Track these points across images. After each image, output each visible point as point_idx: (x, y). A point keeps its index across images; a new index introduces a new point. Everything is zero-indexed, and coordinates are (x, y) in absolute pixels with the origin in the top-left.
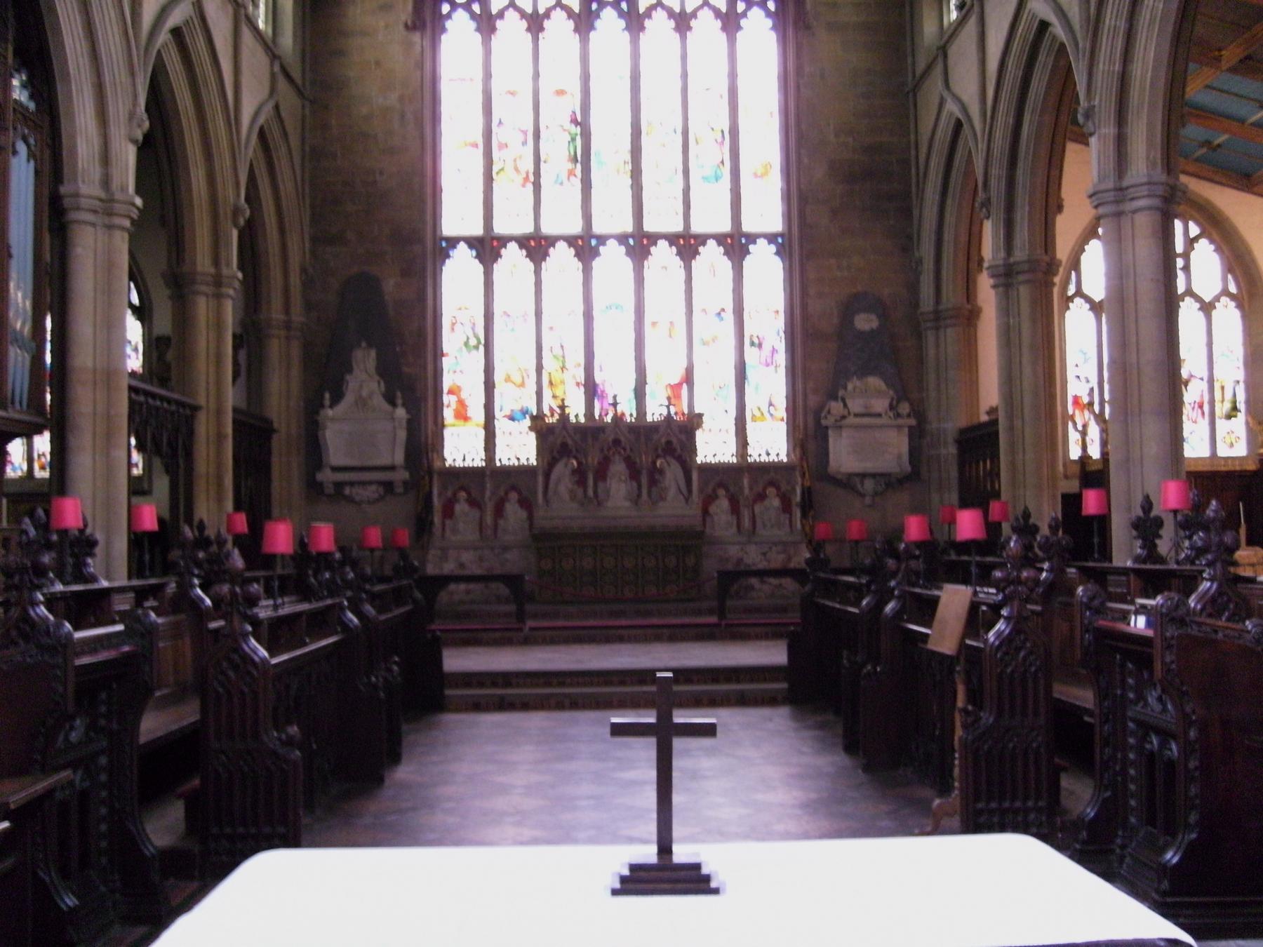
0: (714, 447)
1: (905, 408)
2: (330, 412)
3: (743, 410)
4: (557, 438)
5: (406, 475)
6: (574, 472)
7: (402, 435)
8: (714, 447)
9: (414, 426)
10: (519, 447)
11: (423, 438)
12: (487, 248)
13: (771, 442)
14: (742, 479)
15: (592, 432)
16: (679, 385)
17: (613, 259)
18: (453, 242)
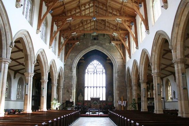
0: (101, 99)
3: (103, 98)
4: (92, 99)
8: (101, 99)
10: (89, 99)
12: (88, 87)
13: (104, 99)
14: (103, 101)
15: (94, 98)
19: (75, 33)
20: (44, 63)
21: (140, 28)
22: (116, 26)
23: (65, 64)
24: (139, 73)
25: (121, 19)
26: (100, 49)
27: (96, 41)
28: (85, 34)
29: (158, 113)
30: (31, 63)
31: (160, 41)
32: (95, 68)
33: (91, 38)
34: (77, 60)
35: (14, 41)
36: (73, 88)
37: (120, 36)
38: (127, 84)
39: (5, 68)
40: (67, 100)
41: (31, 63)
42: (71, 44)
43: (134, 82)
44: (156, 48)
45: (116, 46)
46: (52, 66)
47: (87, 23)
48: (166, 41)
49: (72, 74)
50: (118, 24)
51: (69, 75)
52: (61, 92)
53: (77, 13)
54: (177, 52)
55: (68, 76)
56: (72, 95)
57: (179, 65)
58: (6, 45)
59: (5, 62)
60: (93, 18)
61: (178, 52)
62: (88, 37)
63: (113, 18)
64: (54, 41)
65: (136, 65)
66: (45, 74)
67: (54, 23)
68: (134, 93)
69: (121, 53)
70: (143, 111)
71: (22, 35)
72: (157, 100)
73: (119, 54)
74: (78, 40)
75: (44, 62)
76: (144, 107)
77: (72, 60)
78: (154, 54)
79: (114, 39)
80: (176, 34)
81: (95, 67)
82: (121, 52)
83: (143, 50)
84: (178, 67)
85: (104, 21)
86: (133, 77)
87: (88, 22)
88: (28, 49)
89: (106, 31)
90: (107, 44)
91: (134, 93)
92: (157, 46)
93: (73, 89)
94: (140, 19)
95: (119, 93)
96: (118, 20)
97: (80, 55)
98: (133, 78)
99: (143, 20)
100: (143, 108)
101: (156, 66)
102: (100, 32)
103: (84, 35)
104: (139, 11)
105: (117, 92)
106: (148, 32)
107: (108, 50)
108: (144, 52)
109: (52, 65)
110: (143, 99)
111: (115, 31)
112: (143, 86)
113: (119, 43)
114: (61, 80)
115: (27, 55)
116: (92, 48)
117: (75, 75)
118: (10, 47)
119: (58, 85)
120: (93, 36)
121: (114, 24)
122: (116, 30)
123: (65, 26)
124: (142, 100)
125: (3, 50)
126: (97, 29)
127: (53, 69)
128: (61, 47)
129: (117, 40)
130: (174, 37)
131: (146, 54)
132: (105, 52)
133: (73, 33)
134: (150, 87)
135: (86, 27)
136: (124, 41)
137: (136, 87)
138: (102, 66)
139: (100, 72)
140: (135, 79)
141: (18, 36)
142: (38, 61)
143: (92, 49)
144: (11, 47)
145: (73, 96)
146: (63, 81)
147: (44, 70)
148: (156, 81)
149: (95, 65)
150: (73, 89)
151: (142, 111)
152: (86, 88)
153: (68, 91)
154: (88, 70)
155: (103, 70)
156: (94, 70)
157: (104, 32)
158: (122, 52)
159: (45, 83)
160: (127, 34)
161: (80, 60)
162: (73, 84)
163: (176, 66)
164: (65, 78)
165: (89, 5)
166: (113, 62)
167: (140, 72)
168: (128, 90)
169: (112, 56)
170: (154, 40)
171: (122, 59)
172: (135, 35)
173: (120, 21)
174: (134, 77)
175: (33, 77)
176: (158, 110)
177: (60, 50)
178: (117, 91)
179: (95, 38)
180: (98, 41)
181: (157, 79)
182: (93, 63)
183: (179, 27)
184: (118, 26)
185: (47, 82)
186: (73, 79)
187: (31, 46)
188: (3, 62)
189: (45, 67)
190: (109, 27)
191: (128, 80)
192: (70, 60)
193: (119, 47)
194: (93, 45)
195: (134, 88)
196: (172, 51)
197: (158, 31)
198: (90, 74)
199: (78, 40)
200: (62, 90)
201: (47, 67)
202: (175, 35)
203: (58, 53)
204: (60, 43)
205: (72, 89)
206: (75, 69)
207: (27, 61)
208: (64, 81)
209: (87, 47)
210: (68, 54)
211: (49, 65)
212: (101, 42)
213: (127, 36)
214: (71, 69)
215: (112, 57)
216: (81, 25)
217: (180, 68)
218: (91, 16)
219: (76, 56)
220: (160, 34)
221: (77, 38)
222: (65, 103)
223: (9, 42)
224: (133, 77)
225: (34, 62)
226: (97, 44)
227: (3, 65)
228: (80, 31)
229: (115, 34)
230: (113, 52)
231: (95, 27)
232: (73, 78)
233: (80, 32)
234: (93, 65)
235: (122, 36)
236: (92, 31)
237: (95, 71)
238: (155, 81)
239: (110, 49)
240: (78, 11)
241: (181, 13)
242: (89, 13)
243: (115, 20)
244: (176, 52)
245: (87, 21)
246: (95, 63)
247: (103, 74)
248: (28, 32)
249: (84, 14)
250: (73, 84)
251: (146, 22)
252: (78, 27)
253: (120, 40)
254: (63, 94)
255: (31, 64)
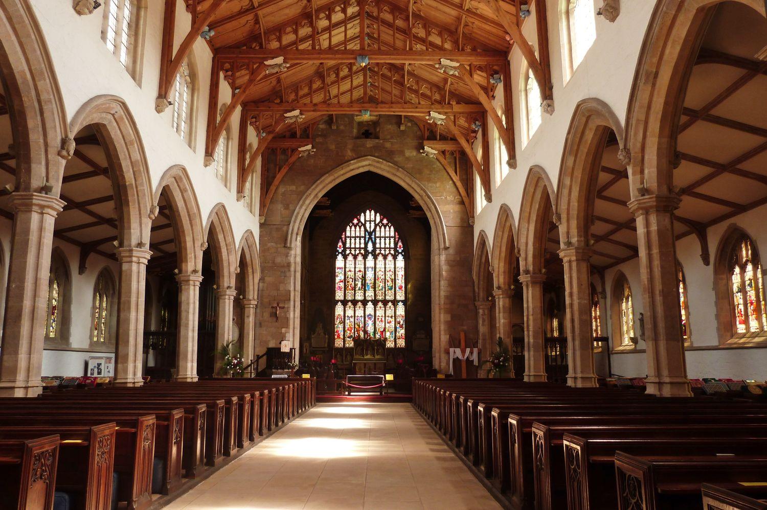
0: (390, 344)
1: (428, 337)
2: (313, 336)
5: (327, 349)
6: (361, 349)
7: (327, 341)
8: (390, 344)
9: (329, 338)
10: (350, 344)
11: (332, 340)
12: (345, 303)
13: (402, 343)
14: (396, 350)
15: (365, 340)
16: (383, 331)
17: (370, 306)
18: (338, 301)
19: (297, 112)
20: (189, 215)
21: (523, 94)
22: (438, 87)
23: (263, 221)
24: (519, 251)
25: (457, 61)
26: (384, 169)
27: (370, 143)
28: (331, 116)
29: (580, 385)
30: (140, 214)
31: (589, 136)
32: (367, 236)
33: (355, 131)
34: (304, 207)
35: (72, 136)
36: (292, 303)
37: (455, 122)
38: (476, 290)
39: (41, 229)
40: (272, 345)
41: (140, 214)
42: (284, 151)
43: (499, 278)
44: (575, 161)
45: (442, 159)
46: (218, 229)
47: (337, 75)
48: (608, 138)
49: (287, 255)
50: (446, 80)
51: (279, 260)
52: (248, 317)
53: (303, 40)
54: (646, 171)
55: (273, 262)
56: (287, 326)
57: (653, 219)
58: (43, 150)
59: (42, 207)
60: (359, 59)
61: (649, 173)
62: (342, 127)
63: (429, 60)
64: (221, 141)
65: (508, 224)
66: (190, 256)
67: (222, 75)
68: (502, 321)
69: (459, 184)
70: (532, 380)
71: (104, 115)
72: (577, 343)
73: (449, 186)
74: (308, 137)
75: (188, 212)
76: (533, 369)
77: (287, 207)
78: (567, 181)
79: (431, 134)
80: (644, 110)
81: (370, 234)
82: (456, 178)
83: (531, 170)
84: (647, 225)
85: (398, 69)
86: (496, 266)
87: (342, 74)
88: (125, 165)
89: (406, 106)
90: (411, 153)
91: (502, 321)
92: (579, 155)
93: (292, 308)
94: (525, 63)
95: (449, 319)
96: (446, 67)
97: (315, 192)
98: (496, 270)
99: (532, 64)
100: (532, 370)
101: (574, 223)
102: (385, 111)
103: (330, 120)
104: (520, 32)
105: (442, 319)
106: (549, 106)
107: (410, 173)
108: (536, 176)
109: (217, 224)
110: (531, 340)
111: (437, 106)
112: (531, 298)
113: (448, 147)
114: (251, 277)
115: (125, 187)
116: (357, 165)
117: (299, 259)
118: (59, 154)
119: (238, 294)
120: (360, 124)
121: (435, 79)
122: (439, 103)
123: (260, 89)
124: (529, 343)
125: (33, 166)
126: (373, 101)
127: (221, 237)
128: (247, 162)
129: (443, 138)
130: (638, 120)
131: (541, 184)
132: (402, 180)
133: (290, 111)
134: (553, 303)
135: (334, 91)
136: (468, 141)
137: (507, 300)
138: (392, 228)
139: (387, 252)
140: (504, 272)
141: (84, 119)
142: (167, 211)
143: (358, 168)
144: (63, 157)
145: (291, 331)
146: (256, 281)
147: (189, 240)
148: (575, 275)
149: (370, 227)
150: (292, 308)
151: (526, 379)
152: (340, 303)
153: (274, 315)
154: (344, 244)
155: (396, 244)
156: (366, 244)
157: (397, 111)
158: (462, 180)
159: (192, 288)
160: (479, 115)
161: (316, 207)
162: (292, 289)
163: (640, 222)
164: (262, 271)
165: (344, 11)
166: (429, 215)
167: (522, 248)
168: (481, 311)
169: (425, 192)
170: (569, 133)
171: (462, 203)
172: (507, 118)
173: (455, 68)
174: (502, 264)
175: (146, 262)
176: (579, 375)
177: (243, 172)
178: (442, 316)
179: (368, 132)
180: (377, 141)
181: (579, 271)
182: (362, 220)
183: (654, 85)
184: (447, 87)
185: (198, 284)
186: (293, 273)
187: (136, 156)
188: (35, 208)
189: (192, 230)
190: (416, 92)
191: (481, 278)
192: (279, 207)
193: (450, 163)
194: (359, 156)
195: (501, 302)
196: (630, 171)
197: (584, 101)
198: (350, 258)
199: (308, 137)
200: (252, 311)
201: (197, 229)
202: (639, 114)
203: (238, 184)
204: (243, 147)
205: (289, 308)
206: (299, 238)
207: (125, 209)
208: (262, 279)
209: (341, 162)
210: (273, 188)
211: (204, 223)
212: (388, 145)
213: (477, 122)
214: (284, 241)
215: (426, 198)
216: (317, 84)
217: (654, 228)
218: (352, 52)
219: (301, 195)
220: (589, 111)
221: (306, 133)
222: (263, 355)
223: (55, 138)
224: (498, 267)
225: (152, 211)
226: (375, 152)
227: (35, 217)
228: (315, 105)
229: (437, 117)
230: (429, 180)
231: (365, 93)
232: (292, 269)
233: (313, 111)
234: (362, 228)
235: (462, 121)
236: (356, 108)
237: (370, 247)
238: (571, 278)
239: (419, 170)
240: (304, 31)
241: (665, 31)
242: (345, 42)
243: (437, 66)
244: (642, 172)
245: (337, 69)
246: (368, 219)
247: (395, 257)
248: (124, 105)
249: (325, 44)
250: (292, 289)
251: (544, 70)
252: (306, 90)
253: (454, 139)
254: (258, 325)
255: (140, 218)
